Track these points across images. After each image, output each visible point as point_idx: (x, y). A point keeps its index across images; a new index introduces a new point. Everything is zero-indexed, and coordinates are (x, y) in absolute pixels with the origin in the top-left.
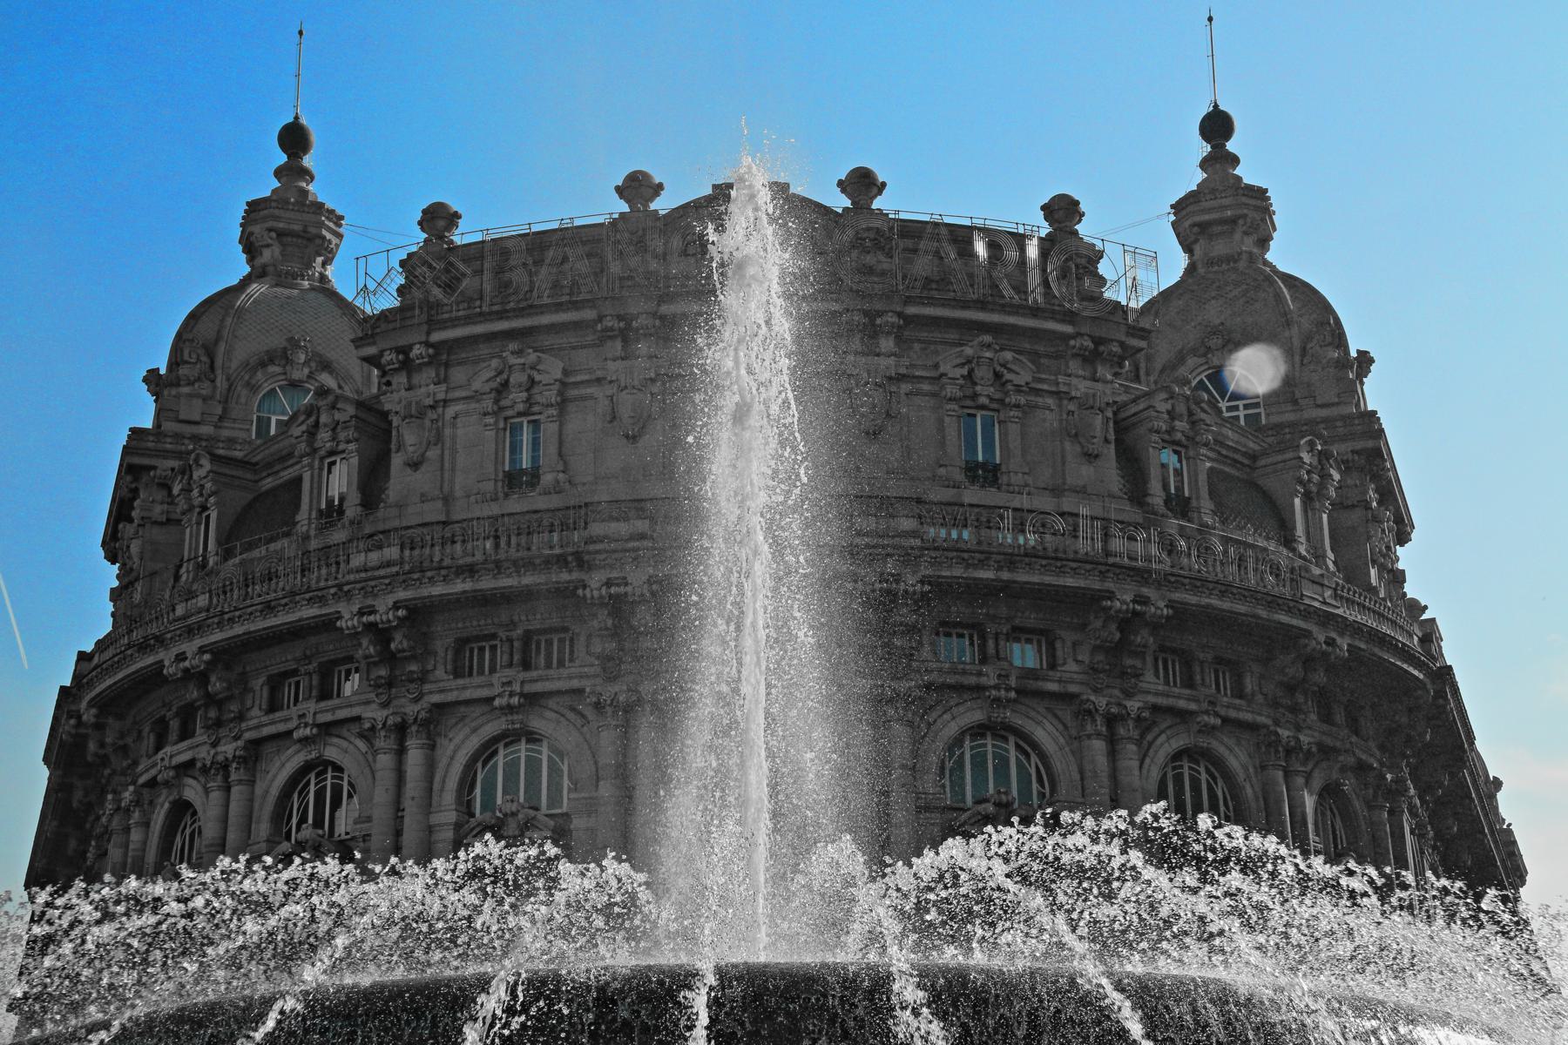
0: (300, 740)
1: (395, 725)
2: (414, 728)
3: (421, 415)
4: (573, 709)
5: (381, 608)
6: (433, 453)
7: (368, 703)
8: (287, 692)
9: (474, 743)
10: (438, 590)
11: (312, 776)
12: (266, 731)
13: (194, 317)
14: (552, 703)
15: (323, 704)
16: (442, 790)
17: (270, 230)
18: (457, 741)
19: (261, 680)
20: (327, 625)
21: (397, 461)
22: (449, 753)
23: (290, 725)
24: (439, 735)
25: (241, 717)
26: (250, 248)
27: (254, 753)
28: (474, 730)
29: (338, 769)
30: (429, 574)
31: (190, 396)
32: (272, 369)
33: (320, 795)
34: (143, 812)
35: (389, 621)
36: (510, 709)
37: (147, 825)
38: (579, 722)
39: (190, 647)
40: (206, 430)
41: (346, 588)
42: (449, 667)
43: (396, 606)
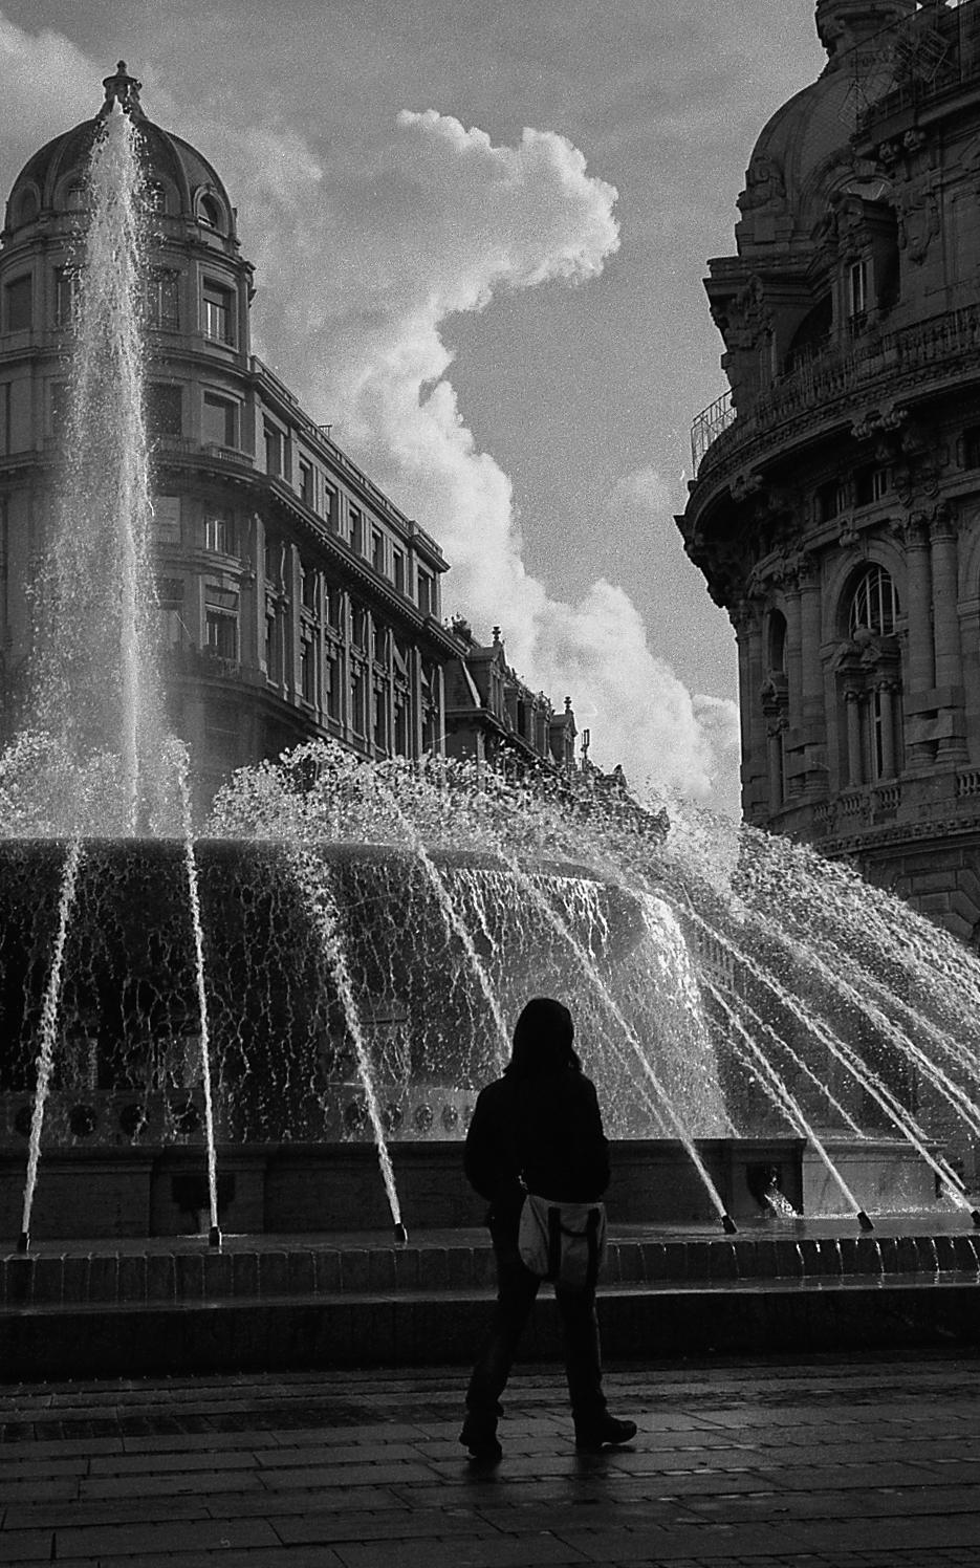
0: (846, 547)
3: (920, 205)
5: (884, 413)
6: (936, 243)
7: (896, 504)
8: (840, 500)
10: (931, 386)
12: (822, 540)
13: (768, 131)
17: (838, 18)
19: (813, 494)
20: (843, 434)
21: (905, 255)
24: (961, 527)
25: (801, 531)
26: (829, 43)
27: (818, 558)
29: (884, 570)
30: (921, 372)
31: (764, 216)
32: (840, 170)
33: (874, 593)
34: (757, 624)
35: (892, 424)
37: (760, 633)
39: (745, 470)
40: (780, 248)
41: (852, 398)
42: (962, 461)
43: (897, 408)
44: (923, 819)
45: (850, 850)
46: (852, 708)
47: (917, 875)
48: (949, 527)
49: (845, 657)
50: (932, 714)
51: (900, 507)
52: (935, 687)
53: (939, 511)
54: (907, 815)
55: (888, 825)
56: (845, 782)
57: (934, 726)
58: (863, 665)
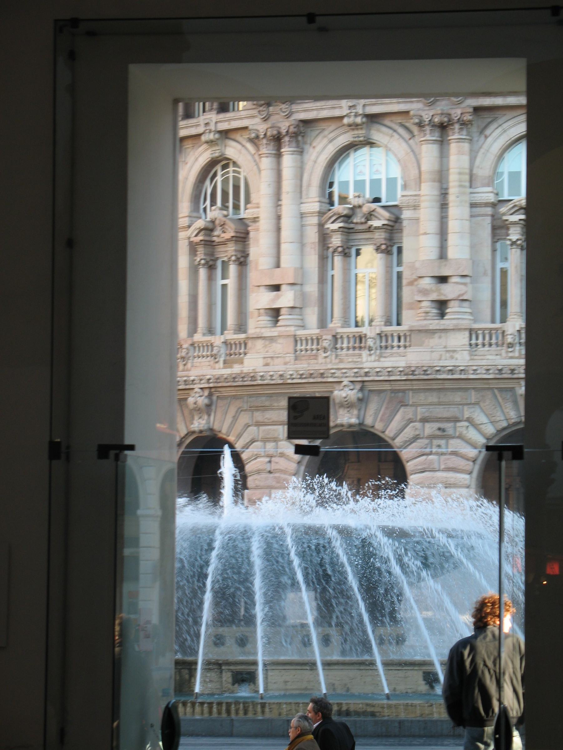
0: (207, 142)
1: (273, 136)
2: (287, 139)
4: (402, 125)
7: (253, 117)
9: (331, 149)
11: (218, 168)
14: (387, 122)
15: (222, 116)
16: (309, 185)
18: (318, 149)
22: (313, 157)
23: (200, 130)
28: (331, 141)
29: (235, 164)
33: (225, 182)
36: (354, 126)
38: (407, 136)
44: (266, 369)
45: (202, 386)
46: (203, 273)
47: (257, 410)
48: (297, 142)
49: (201, 230)
50: (277, 288)
51: (257, 120)
52: (278, 266)
53: (292, 129)
54: (253, 363)
55: (236, 369)
56: (193, 330)
57: (278, 297)
58: (215, 239)
